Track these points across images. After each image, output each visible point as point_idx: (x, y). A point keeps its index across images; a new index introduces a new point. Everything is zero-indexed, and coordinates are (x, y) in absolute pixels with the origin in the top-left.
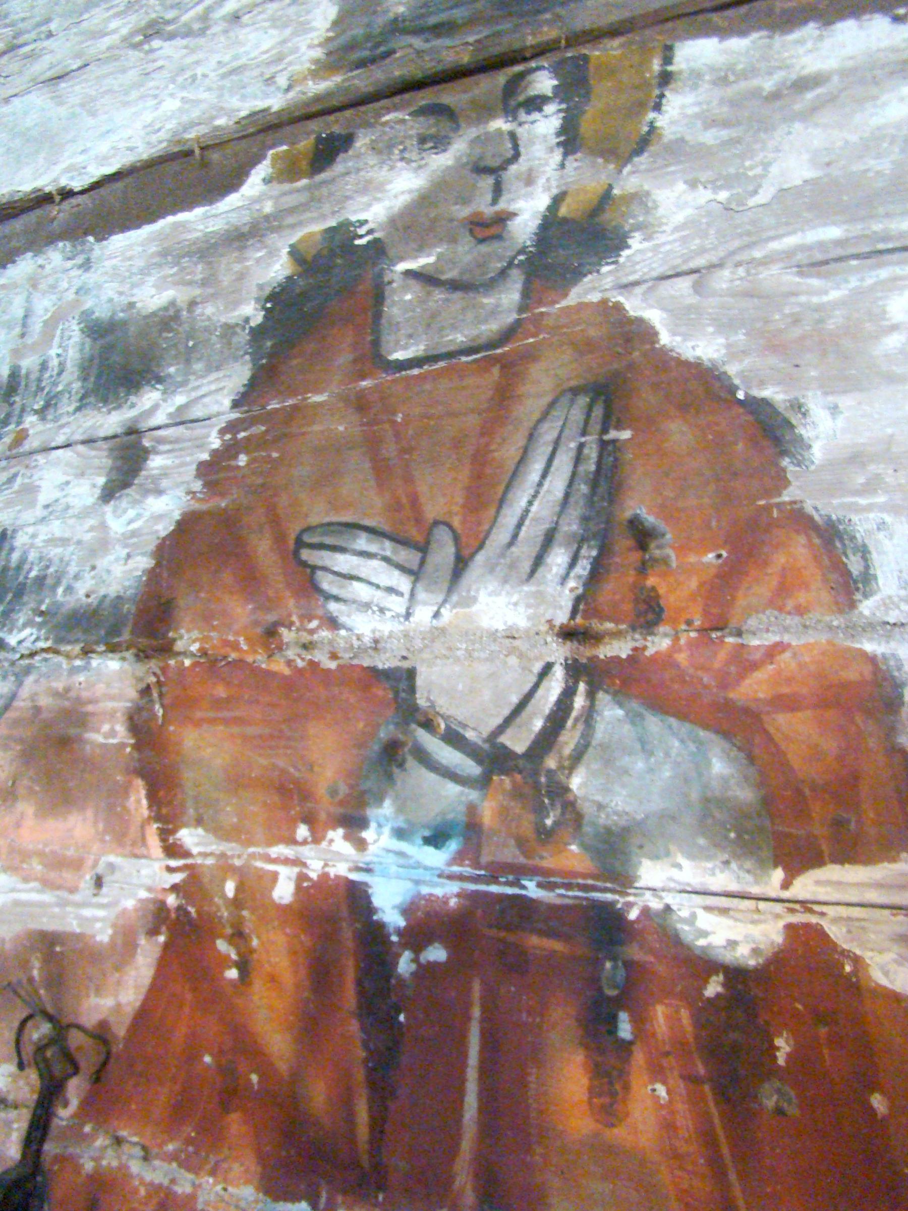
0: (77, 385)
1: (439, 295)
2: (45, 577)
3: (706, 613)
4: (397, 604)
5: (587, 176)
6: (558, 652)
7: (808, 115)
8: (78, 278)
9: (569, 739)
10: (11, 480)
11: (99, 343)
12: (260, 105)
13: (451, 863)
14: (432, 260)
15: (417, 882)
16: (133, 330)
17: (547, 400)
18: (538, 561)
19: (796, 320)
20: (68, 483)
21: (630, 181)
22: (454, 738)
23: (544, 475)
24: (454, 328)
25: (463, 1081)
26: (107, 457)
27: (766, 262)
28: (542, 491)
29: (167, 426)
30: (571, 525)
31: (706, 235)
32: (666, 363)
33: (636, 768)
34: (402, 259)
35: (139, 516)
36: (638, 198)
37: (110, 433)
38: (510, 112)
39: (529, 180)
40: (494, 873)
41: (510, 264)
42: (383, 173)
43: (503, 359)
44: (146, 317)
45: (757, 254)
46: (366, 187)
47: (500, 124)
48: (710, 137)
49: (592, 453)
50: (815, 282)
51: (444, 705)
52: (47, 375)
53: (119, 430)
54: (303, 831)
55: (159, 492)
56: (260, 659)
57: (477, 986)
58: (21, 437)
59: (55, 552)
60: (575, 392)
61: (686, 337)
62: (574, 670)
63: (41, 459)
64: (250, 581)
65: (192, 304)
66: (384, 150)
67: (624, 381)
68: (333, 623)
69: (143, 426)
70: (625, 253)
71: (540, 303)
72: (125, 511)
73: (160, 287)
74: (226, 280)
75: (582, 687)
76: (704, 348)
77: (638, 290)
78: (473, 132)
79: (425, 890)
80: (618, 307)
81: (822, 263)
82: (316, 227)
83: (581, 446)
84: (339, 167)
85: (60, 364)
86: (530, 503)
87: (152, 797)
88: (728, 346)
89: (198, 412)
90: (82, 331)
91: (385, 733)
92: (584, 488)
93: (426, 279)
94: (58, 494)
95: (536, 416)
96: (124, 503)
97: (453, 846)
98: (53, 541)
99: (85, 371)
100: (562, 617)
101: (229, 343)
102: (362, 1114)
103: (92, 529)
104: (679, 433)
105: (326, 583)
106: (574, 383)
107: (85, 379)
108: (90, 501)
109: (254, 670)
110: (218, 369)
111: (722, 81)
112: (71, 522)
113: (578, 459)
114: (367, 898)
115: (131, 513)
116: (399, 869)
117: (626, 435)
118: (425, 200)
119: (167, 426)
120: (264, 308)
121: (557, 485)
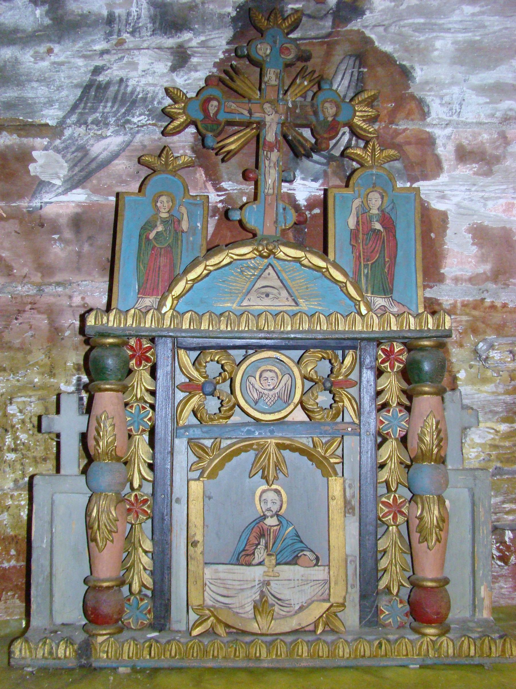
0: (150, 25)
2: (146, 98)
3: (388, 119)
11: (158, 10)
13: (320, 186)
14: (301, 6)
15: (310, 192)
16: (175, 8)
17: (342, 57)
19: (412, 44)
20: (152, 63)
23: (342, 79)
24: (310, 30)
26: (171, 55)
27: (404, 26)
29: (196, 47)
31: (387, 15)
32: (376, 51)
34: (290, 4)
35: (189, 79)
37: (170, 46)
41: (328, 13)
43: (328, 42)
44: (181, 4)
45: (402, 23)
49: (356, 74)
50: (417, 34)
52: (131, 18)
53: (174, 46)
55: (197, 71)
58: (121, 43)
59: (150, 89)
60: (351, 56)
61: (382, 44)
63: (136, 52)
69: (186, 46)
70: (365, 16)
71: (338, 27)
72: (183, 76)
75: (354, 138)
76: (387, 48)
77: (369, 28)
79: (313, 194)
80: (363, 33)
81: (419, 29)
83: (352, 72)
85: (138, 15)
86: (338, 87)
87: (207, 175)
88: (394, 49)
89: (211, 44)
90: (148, 3)
92: (354, 84)
94: (149, 67)
95: (339, 61)
96: (182, 73)
97: (321, 181)
98: (149, 85)
99: (153, 19)
101: (222, 21)
103: (167, 81)
104: (380, 71)
106: (349, 53)
107: (154, 23)
108: (165, 71)
110: (218, 29)
112: (157, 78)
113: (352, 75)
114: (295, 197)
115: (186, 77)
117: (366, 70)
119: (196, 47)
120: (236, 10)
121: (346, 82)
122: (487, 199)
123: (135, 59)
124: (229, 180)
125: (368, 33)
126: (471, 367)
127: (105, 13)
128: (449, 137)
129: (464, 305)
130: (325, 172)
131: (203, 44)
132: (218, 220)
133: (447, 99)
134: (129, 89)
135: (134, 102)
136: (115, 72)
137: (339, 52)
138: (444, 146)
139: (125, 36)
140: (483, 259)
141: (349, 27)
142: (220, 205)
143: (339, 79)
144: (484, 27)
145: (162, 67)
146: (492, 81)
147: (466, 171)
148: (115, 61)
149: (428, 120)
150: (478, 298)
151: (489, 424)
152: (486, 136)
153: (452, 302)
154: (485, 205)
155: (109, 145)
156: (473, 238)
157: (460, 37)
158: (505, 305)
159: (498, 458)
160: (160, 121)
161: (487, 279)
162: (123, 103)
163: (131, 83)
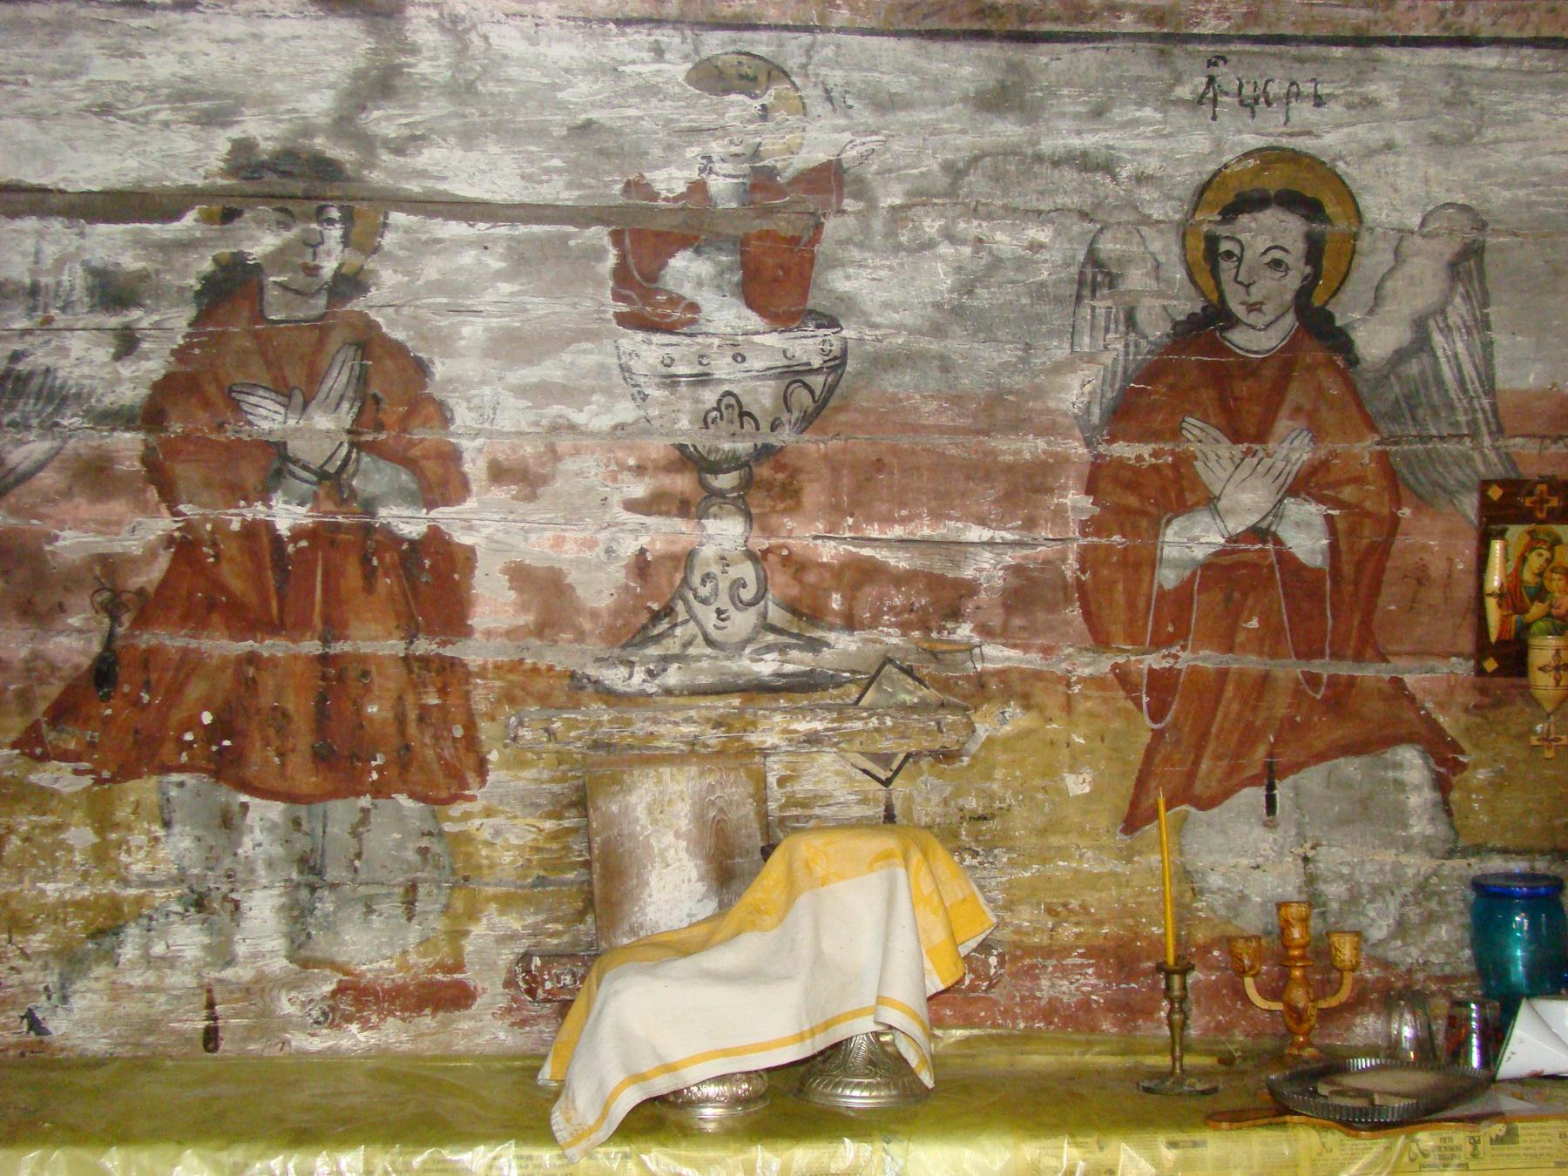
0: (86, 299)
1: (290, 295)
4: (280, 418)
5: (354, 259)
6: (345, 438)
7: (437, 253)
8: (77, 241)
9: (351, 468)
10: (47, 342)
12: (193, 182)
18: (338, 405)
19: (431, 330)
21: (371, 264)
22: (305, 468)
25: (314, 586)
28: (338, 379)
30: (350, 393)
32: (385, 339)
33: (374, 477)
36: (374, 272)
38: (320, 222)
39: (329, 254)
40: (326, 514)
42: (258, 233)
43: (321, 327)
46: (251, 238)
47: (314, 226)
48: (402, 253)
49: (357, 368)
51: (300, 455)
54: (242, 503)
56: (213, 437)
57: (320, 555)
58: (49, 320)
62: (352, 445)
64: (207, 404)
65: (157, 272)
66: (260, 222)
67: (368, 341)
68: (251, 424)
73: (137, 258)
74: (177, 265)
76: (399, 335)
78: (303, 226)
82: (226, 250)
84: (237, 223)
89: (167, 325)
91: (276, 464)
93: (283, 286)
99: (91, 292)
100: (348, 426)
102: (274, 604)
104: (389, 364)
105: (245, 407)
108: (106, 359)
109: (211, 440)
111: (406, 232)
116: (287, 515)
118: (281, 251)
121: (344, 378)
122: (527, 531)
123: (67, 343)
124: (190, 502)
125: (373, 315)
126: (506, 746)
127: (27, 281)
128: (480, 450)
129: (497, 667)
130: (315, 496)
131: (157, 326)
132: (175, 553)
133: (476, 401)
134: (58, 382)
135: (64, 399)
136: (39, 359)
137: (335, 341)
138: (473, 461)
139: (53, 312)
140: (523, 607)
141: (348, 307)
142: (177, 534)
143: (335, 374)
144: (525, 310)
145: (103, 354)
146: (534, 380)
147: (501, 494)
148: (40, 345)
149: (452, 428)
150: (516, 658)
151: (529, 820)
152: (529, 449)
153: (480, 661)
154: (526, 540)
155: (31, 453)
156: (510, 581)
157: (494, 322)
158: (551, 668)
159: (542, 864)
160: (98, 423)
161: (531, 633)
162: (50, 400)
163: (60, 374)
